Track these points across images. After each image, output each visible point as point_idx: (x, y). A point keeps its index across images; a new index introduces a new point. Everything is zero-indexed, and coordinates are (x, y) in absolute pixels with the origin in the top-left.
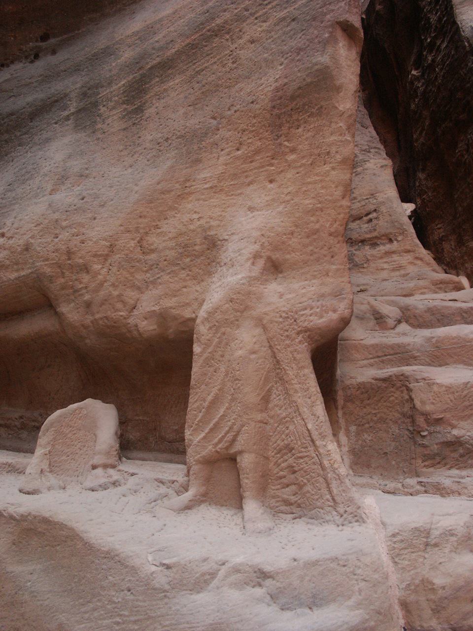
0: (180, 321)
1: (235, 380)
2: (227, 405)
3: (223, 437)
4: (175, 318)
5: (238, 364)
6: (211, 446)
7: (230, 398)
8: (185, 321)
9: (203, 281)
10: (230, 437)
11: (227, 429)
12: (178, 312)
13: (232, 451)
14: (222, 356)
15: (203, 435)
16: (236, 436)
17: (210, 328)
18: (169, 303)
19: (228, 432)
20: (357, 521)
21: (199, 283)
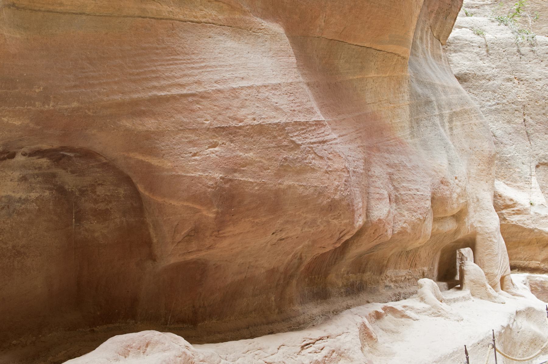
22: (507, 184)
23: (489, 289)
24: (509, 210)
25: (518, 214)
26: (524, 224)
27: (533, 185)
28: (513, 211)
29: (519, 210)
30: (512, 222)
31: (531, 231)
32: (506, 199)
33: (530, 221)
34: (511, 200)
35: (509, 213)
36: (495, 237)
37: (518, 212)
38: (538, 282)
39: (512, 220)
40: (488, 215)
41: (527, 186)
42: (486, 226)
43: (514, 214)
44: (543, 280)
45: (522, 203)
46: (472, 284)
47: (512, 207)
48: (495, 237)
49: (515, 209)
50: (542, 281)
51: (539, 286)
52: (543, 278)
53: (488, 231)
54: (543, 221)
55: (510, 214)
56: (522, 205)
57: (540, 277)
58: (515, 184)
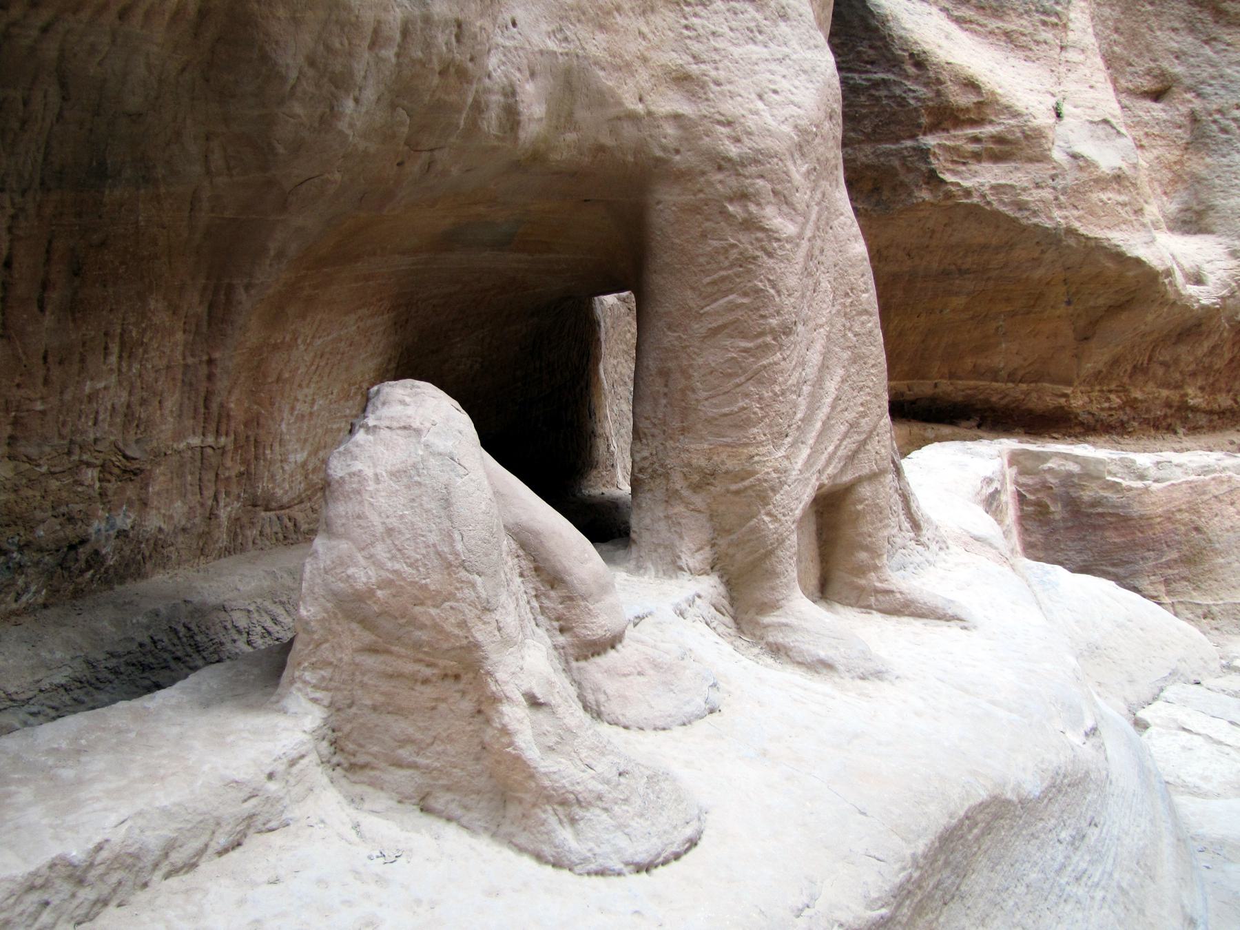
0: (613, 112)
1: (860, 313)
2: (841, 372)
3: (837, 448)
4: (601, 98)
5: (863, 275)
6: (815, 477)
7: (846, 355)
8: (619, 118)
9: (653, 10)
10: (849, 445)
11: (843, 428)
12: (610, 84)
13: (847, 478)
14: (822, 251)
15: (805, 452)
16: (864, 443)
17: (809, 172)
18: (596, 44)
19: (846, 436)
20: (941, 549)
21: (644, 12)
22: (959, 21)
23: (515, 715)
24: (959, 137)
25: (996, 158)
26: (1021, 206)
27: (1072, 36)
28: (976, 140)
29: (999, 140)
30: (968, 193)
31: (1053, 239)
32: (945, 76)
33: (1046, 194)
34: (971, 85)
35: (955, 150)
36: (783, 199)
37: (1004, 149)
38: (1052, 480)
39: (966, 184)
40: (753, 34)
41: (1046, 35)
42: (729, 108)
43: (977, 157)
44: (1074, 468)
45: (1020, 106)
46: (353, 637)
47: (973, 123)
48: (783, 199)
49: (988, 130)
50: (1070, 475)
51: (1055, 498)
52: (1075, 459)
53: (733, 151)
54: (1104, 196)
55: (959, 158)
56: (1016, 114)
57: (1066, 457)
58: (993, 24)
